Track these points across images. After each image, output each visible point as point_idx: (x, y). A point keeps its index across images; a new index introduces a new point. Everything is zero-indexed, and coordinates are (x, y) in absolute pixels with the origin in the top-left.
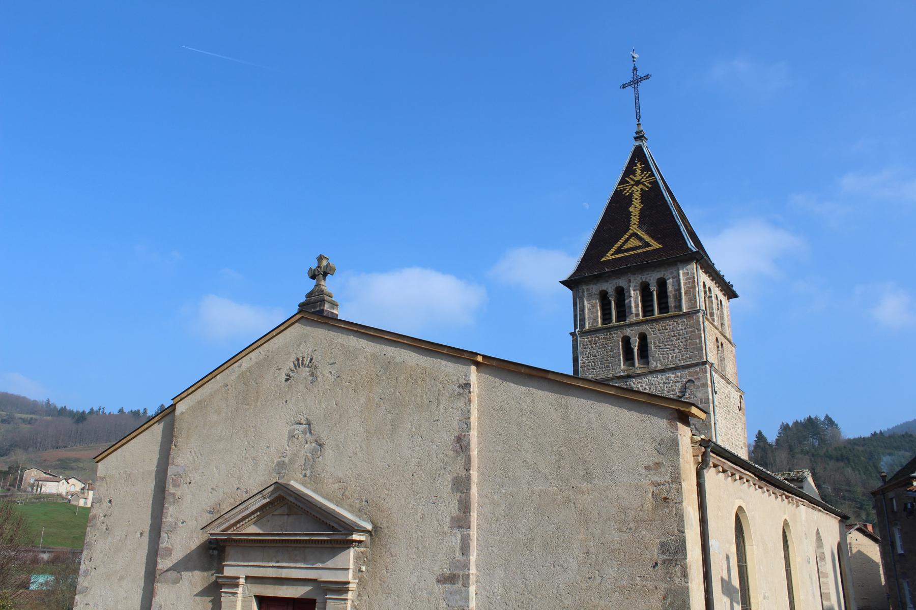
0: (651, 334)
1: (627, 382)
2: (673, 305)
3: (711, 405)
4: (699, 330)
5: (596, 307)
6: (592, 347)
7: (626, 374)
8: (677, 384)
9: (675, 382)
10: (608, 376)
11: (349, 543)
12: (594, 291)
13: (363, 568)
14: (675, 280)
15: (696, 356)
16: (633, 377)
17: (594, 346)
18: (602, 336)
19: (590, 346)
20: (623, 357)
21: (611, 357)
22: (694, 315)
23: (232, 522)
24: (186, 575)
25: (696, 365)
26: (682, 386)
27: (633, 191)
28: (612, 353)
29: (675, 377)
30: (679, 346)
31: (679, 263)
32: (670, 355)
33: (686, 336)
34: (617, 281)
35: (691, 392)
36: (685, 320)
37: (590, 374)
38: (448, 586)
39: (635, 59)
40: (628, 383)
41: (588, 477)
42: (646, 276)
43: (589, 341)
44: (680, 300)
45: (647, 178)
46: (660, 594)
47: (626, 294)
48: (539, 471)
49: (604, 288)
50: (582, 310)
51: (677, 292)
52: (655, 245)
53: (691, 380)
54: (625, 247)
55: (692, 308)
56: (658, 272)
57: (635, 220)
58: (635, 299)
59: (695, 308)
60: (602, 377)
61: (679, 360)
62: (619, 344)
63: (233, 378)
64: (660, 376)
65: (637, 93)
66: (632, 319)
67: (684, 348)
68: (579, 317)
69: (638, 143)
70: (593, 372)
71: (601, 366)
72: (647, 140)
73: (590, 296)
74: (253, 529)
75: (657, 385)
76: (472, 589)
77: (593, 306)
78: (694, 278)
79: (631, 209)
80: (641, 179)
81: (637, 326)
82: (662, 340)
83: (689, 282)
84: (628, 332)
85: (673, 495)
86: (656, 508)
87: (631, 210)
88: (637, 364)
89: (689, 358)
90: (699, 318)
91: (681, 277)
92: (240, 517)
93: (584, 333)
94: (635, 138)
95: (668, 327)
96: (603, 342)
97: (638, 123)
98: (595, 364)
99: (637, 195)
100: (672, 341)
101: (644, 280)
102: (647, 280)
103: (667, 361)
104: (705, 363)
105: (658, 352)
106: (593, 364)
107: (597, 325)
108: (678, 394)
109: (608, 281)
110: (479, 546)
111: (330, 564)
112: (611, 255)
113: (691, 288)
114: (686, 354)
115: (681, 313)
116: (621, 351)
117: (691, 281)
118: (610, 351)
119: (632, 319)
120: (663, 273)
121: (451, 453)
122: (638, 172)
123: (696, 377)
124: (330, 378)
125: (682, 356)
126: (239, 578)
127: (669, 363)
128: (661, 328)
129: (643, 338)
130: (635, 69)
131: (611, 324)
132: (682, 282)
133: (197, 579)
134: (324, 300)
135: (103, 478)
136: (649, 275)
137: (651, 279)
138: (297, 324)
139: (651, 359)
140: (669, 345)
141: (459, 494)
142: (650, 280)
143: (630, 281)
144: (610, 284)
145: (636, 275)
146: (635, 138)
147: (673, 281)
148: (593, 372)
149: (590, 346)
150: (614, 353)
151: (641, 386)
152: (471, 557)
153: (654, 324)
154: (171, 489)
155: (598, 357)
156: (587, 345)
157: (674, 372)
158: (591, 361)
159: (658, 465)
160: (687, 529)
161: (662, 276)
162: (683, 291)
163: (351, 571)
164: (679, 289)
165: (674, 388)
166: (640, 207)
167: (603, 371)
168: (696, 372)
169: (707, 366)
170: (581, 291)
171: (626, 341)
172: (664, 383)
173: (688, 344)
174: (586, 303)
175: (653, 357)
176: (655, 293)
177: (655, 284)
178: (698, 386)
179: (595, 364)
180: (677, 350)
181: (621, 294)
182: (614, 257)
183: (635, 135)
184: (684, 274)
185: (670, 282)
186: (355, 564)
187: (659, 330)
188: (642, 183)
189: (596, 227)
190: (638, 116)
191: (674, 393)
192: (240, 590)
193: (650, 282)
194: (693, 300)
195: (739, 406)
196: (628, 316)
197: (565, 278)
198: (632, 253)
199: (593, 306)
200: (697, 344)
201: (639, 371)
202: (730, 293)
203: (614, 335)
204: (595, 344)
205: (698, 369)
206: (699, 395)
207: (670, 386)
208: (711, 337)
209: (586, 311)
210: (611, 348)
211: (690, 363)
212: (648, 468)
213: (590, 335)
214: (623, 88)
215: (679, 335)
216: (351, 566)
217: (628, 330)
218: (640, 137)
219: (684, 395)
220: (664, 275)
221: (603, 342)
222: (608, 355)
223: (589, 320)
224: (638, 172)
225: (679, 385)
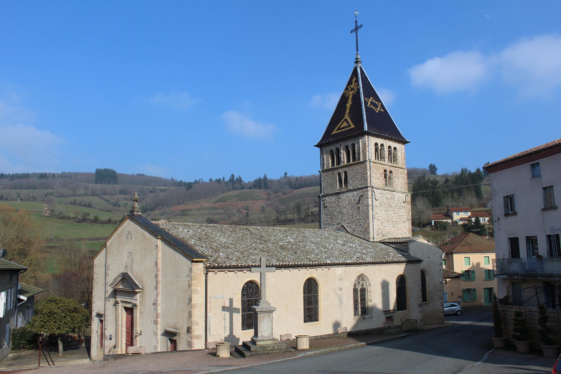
2: (357, 157)
3: (370, 208)
4: (366, 170)
5: (329, 158)
6: (327, 178)
7: (339, 192)
9: (356, 196)
10: (333, 192)
11: (137, 293)
13: (141, 300)
15: (365, 183)
16: (341, 193)
19: (326, 178)
20: (339, 183)
23: (115, 284)
24: (111, 299)
25: (364, 188)
27: (350, 94)
36: (361, 165)
38: (154, 306)
39: (356, 16)
41: (178, 277)
42: (347, 143)
43: (326, 175)
45: (356, 86)
46: (187, 313)
47: (340, 152)
48: (170, 274)
50: (323, 160)
52: (353, 126)
53: (362, 195)
54: (341, 127)
55: (364, 159)
57: (348, 111)
59: (365, 159)
60: (330, 193)
62: (337, 177)
63: (117, 235)
64: (351, 193)
65: (357, 36)
66: (342, 164)
67: (361, 179)
68: (322, 165)
69: (356, 65)
72: (361, 62)
74: (121, 287)
76: (159, 307)
77: (328, 158)
78: (365, 144)
79: (347, 105)
80: (354, 87)
84: (340, 171)
85: (190, 285)
86: (188, 288)
89: (362, 184)
90: (366, 164)
92: (117, 283)
93: (324, 171)
94: (355, 62)
95: (355, 169)
97: (357, 53)
99: (351, 97)
102: (348, 145)
104: (367, 187)
107: (329, 167)
108: (357, 202)
109: (333, 145)
110: (161, 295)
111: (134, 298)
112: (336, 131)
113: (364, 149)
115: (359, 162)
116: (338, 180)
117: (364, 145)
119: (342, 164)
120: (354, 141)
121: (155, 266)
123: (364, 194)
124: (134, 239)
126: (118, 301)
129: (346, 173)
130: (356, 22)
131: (334, 167)
132: (361, 146)
133: (112, 301)
134: (134, 211)
135: (95, 265)
138: (128, 219)
141: (156, 279)
142: (349, 144)
143: (341, 145)
145: (343, 143)
146: (355, 62)
151: (344, 197)
152: (158, 298)
154: (107, 272)
157: (356, 191)
159: (189, 275)
160: (194, 294)
161: (353, 142)
162: (361, 150)
163: (138, 301)
164: (359, 150)
165: (356, 199)
166: (351, 104)
168: (364, 191)
169: (369, 188)
170: (323, 150)
171: (339, 174)
172: (352, 196)
174: (325, 156)
176: (351, 151)
177: (351, 147)
178: (365, 198)
181: (338, 151)
182: (336, 132)
183: (355, 61)
184: (362, 141)
185: (356, 145)
186: (140, 298)
189: (332, 115)
192: (120, 305)
193: (349, 146)
194: (365, 155)
195: (405, 200)
197: (316, 145)
198: (343, 130)
199: (327, 158)
201: (344, 190)
202: (404, 142)
204: (328, 176)
205: (365, 190)
206: (365, 202)
208: (378, 171)
209: (325, 160)
211: (362, 187)
212: (187, 276)
214: (352, 33)
215: (359, 173)
216: (138, 299)
218: (357, 62)
219: (359, 202)
222: (332, 182)
225: (358, 197)
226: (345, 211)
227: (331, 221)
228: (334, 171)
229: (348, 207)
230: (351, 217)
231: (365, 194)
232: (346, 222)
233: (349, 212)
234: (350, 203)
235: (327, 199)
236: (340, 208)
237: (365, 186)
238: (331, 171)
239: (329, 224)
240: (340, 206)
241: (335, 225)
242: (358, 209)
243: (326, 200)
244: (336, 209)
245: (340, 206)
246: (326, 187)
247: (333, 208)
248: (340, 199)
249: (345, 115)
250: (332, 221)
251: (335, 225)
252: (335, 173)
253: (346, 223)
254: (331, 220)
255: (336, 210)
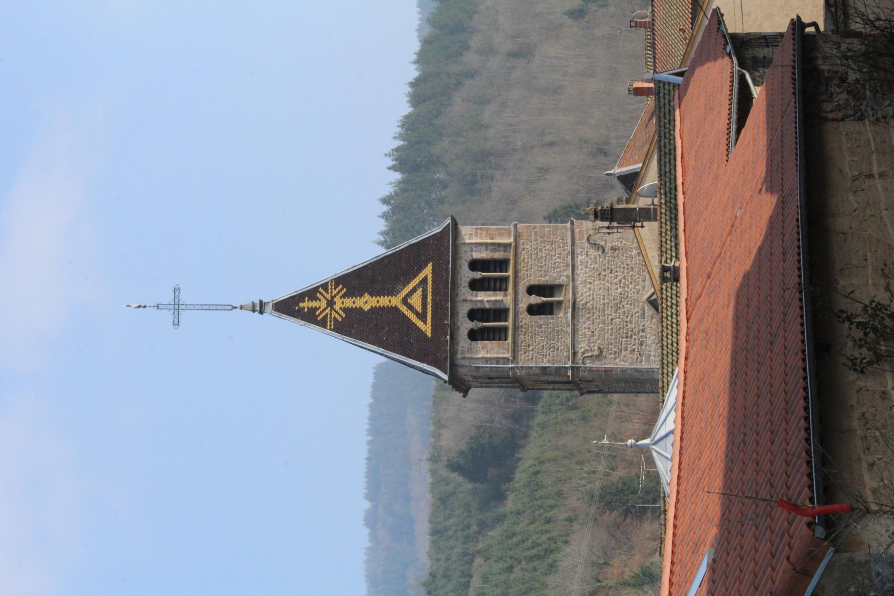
0: (530, 280)
1: (579, 309)
6: (533, 350)
8: (590, 253)
9: (587, 255)
12: (467, 346)
14: (474, 249)
15: (563, 233)
17: (531, 348)
18: (522, 337)
19: (531, 352)
21: (548, 328)
22: (518, 231)
26: (593, 248)
28: (543, 326)
29: (582, 255)
30: (549, 250)
31: (458, 242)
32: (556, 261)
33: (539, 241)
34: (461, 315)
35: (600, 239)
37: (563, 354)
40: (581, 307)
43: (525, 353)
44: (499, 245)
49: (466, 332)
51: (489, 248)
52: (427, 271)
53: (588, 237)
56: (461, 268)
57: (384, 301)
58: (485, 298)
61: (564, 250)
64: (578, 271)
67: (552, 244)
69: (269, 308)
70: (561, 350)
71: (555, 340)
73: (470, 350)
75: (587, 275)
79: (366, 308)
81: (518, 295)
82: (539, 268)
83: (480, 233)
87: (369, 307)
88: (561, 299)
89: (563, 240)
91: (474, 241)
95: (526, 261)
96: (528, 336)
98: (552, 347)
99: (349, 303)
100: (542, 257)
101: (467, 284)
102: (468, 280)
103: (563, 264)
105: (551, 274)
106: (552, 350)
108: (600, 253)
109: (459, 328)
113: (487, 232)
114: (559, 242)
115: (513, 244)
118: (541, 328)
122: (314, 304)
123: (585, 233)
125: (560, 247)
127: (565, 262)
128: (525, 268)
129: (532, 290)
132: (479, 241)
136: (463, 277)
137: (468, 275)
139: (557, 282)
140: (546, 260)
142: (468, 277)
144: (462, 324)
145: (460, 293)
147: (476, 251)
148: (561, 350)
149: (531, 352)
150: (543, 324)
151: (586, 293)
153: (520, 275)
155: (545, 343)
156: (528, 356)
157: (576, 255)
158: (548, 352)
161: (467, 264)
162: (490, 241)
164: (486, 245)
165: (592, 257)
167: (561, 338)
168: (579, 232)
171: (533, 310)
173: (548, 240)
174: (480, 356)
175: (556, 279)
179: (552, 347)
180: (553, 253)
184: (469, 238)
185: (476, 255)
187: (527, 271)
188: (333, 297)
190: (228, 308)
191: (598, 257)
196: (504, 305)
200: (550, 231)
203: (523, 323)
205: (577, 230)
207: (590, 261)
209: (488, 356)
210: (538, 327)
213: (518, 352)
217: (520, 305)
218: (260, 308)
219: (602, 247)
220: (466, 260)
221: (528, 336)
223: (499, 354)
224: (314, 304)
226: (617, 289)
227: (634, 337)
228: (521, 324)
229: (608, 282)
230: (631, 273)
231: (587, 230)
232: (641, 289)
233: (619, 278)
234: (600, 274)
235: (582, 347)
236: (608, 307)
237: (569, 233)
238: (519, 335)
239: (641, 344)
240: (604, 304)
241: (644, 325)
242: (615, 250)
243: (583, 353)
244: (610, 317)
245: (604, 304)
246: (553, 357)
247: (606, 328)
248: (586, 303)
249: (392, 306)
250: (635, 334)
251: (644, 325)
252: (525, 324)
253: (644, 287)
254: (631, 337)
255: (612, 320)
